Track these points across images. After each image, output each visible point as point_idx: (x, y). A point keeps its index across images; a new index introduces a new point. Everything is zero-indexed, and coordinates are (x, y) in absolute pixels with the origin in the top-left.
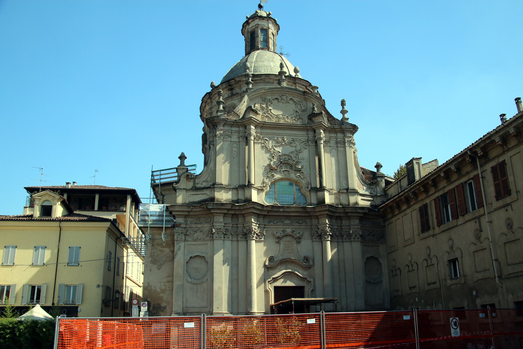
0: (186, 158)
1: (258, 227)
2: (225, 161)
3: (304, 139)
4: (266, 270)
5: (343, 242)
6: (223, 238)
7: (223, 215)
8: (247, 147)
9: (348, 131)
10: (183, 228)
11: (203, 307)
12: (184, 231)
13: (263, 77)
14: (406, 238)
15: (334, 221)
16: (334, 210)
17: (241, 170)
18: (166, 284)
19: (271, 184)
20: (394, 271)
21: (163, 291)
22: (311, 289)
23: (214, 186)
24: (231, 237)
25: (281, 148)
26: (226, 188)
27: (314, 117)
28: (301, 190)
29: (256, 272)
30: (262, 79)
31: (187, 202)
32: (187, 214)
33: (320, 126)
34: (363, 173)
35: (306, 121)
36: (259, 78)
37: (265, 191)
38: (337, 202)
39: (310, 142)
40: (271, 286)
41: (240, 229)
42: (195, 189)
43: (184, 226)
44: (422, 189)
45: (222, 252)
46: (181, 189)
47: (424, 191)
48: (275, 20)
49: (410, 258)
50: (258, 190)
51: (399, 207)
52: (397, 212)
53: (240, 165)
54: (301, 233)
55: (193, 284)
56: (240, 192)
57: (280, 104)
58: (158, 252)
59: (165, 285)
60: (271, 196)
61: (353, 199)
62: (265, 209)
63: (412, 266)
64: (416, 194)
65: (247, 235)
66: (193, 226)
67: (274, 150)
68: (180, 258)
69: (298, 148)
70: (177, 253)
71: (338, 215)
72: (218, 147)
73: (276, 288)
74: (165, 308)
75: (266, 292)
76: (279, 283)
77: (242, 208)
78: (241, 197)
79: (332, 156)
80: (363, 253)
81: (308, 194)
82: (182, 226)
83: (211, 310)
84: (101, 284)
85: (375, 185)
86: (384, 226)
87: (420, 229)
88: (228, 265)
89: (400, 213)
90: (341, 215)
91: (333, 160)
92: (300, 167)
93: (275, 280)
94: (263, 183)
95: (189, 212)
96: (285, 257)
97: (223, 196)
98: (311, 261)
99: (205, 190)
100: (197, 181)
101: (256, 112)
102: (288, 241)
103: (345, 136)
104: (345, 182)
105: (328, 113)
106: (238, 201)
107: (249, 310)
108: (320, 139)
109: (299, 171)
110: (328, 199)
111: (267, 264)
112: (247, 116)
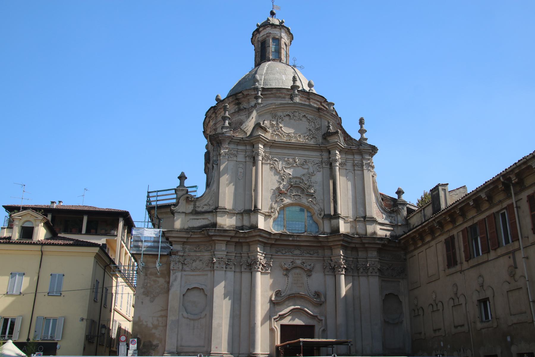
0: (186, 178)
1: (265, 257)
2: (230, 183)
3: (318, 160)
5: (359, 276)
6: (225, 269)
8: (254, 168)
9: (366, 153)
10: (180, 256)
11: (200, 346)
12: (182, 260)
13: (274, 91)
15: (349, 252)
16: (349, 240)
18: (160, 319)
19: (280, 209)
20: (416, 311)
21: (156, 327)
22: (322, 329)
23: (216, 210)
24: (233, 267)
25: (292, 170)
27: (329, 136)
28: (313, 217)
29: (261, 307)
30: (272, 94)
31: (186, 227)
32: (185, 240)
33: (336, 146)
34: (382, 199)
35: (320, 140)
36: (270, 93)
38: (353, 231)
39: (324, 164)
40: (277, 324)
41: (244, 259)
42: (195, 213)
43: (182, 254)
44: (448, 219)
45: (223, 284)
46: (179, 212)
47: (450, 221)
49: (434, 296)
50: (266, 215)
51: (422, 239)
52: (420, 244)
53: (247, 187)
54: (312, 265)
55: (190, 319)
56: (246, 217)
57: (292, 121)
58: (152, 283)
59: (158, 320)
61: (370, 229)
62: (272, 237)
63: (437, 305)
64: (441, 225)
65: (251, 266)
66: (192, 254)
67: (284, 171)
68: (176, 290)
69: (311, 170)
71: (353, 245)
72: (222, 167)
73: (282, 326)
74: (157, 346)
75: (272, 330)
76: (286, 321)
77: (246, 236)
78: (246, 223)
79: (348, 180)
81: (321, 221)
82: (180, 254)
83: (209, 351)
84: (85, 317)
85: (395, 214)
86: (405, 259)
87: (446, 264)
88: (229, 299)
89: (423, 245)
90: (357, 246)
91: (349, 184)
92: (312, 191)
93: (282, 317)
94: (271, 208)
95: (188, 238)
96: (293, 292)
97: (227, 222)
98: (323, 297)
99: (206, 214)
101: (265, 130)
102: (297, 274)
103: (363, 158)
104: (362, 209)
105: (344, 132)
106: (242, 228)
107: (251, 351)
108: (336, 161)
109: (311, 195)
110: (343, 228)
111: (273, 299)
112: (256, 134)
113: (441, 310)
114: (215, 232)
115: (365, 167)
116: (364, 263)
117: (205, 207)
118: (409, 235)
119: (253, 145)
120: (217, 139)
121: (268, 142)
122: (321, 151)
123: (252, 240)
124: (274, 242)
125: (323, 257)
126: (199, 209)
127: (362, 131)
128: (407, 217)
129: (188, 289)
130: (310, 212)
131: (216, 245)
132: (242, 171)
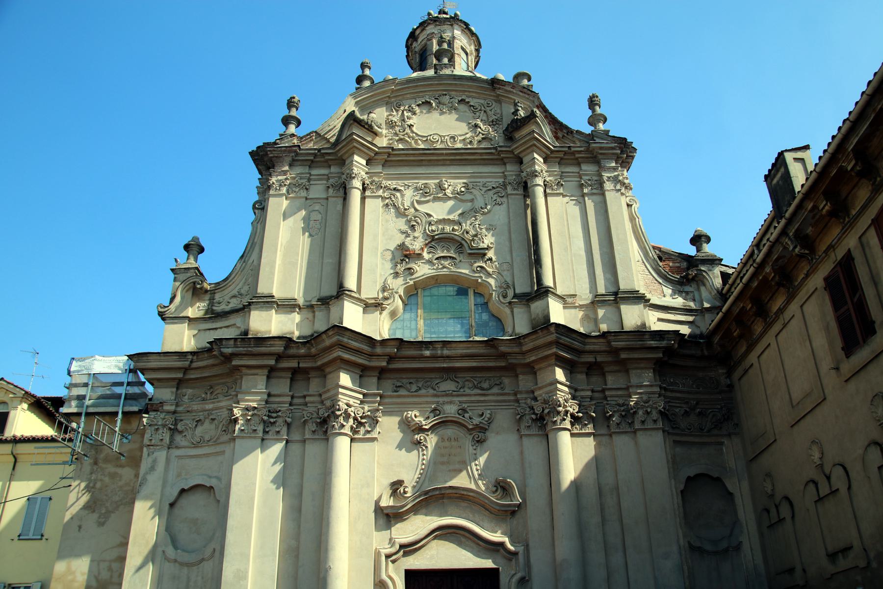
4: (382, 521)
6: (261, 434)
7: (266, 372)
9: (609, 157)
10: (168, 412)
12: (170, 419)
14: (797, 395)
15: (582, 377)
16: (576, 344)
19: (407, 290)
20: (773, 511)
22: (519, 575)
24: (285, 429)
26: (287, 306)
28: (490, 305)
33: (535, 145)
34: (660, 258)
37: (389, 309)
39: (509, 188)
40: (396, 570)
43: (173, 408)
44: (825, 207)
47: (832, 214)
48: (467, 25)
49: (816, 455)
51: (762, 311)
52: (758, 328)
54: (487, 414)
55: (183, 564)
56: (320, 314)
58: (107, 479)
59: (110, 569)
60: (407, 323)
61: (632, 316)
62: (379, 350)
63: (828, 478)
64: (807, 243)
65: (325, 425)
67: (416, 210)
70: (145, 479)
71: (590, 359)
73: (411, 576)
76: (420, 561)
77: (313, 350)
78: (321, 327)
80: (674, 464)
81: (507, 311)
82: (167, 408)
85: (694, 285)
86: (731, 387)
87: (839, 343)
89: (768, 326)
90: (599, 359)
94: (384, 289)
97: (269, 323)
100: (217, 297)
101: (369, 128)
102: (449, 439)
103: (601, 168)
105: (552, 120)
108: (534, 174)
113: (843, 490)
114: (236, 346)
115: (608, 186)
116: (621, 401)
118: (729, 310)
119: (343, 162)
120: (266, 159)
121: (376, 153)
122: (503, 162)
123: (325, 360)
124: (384, 364)
125: (515, 394)
126: (218, 308)
127: (594, 120)
128: (723, 289)
129: (183, 491)
130: (481, 295)
131: (244, 378)
132: (319, 217)
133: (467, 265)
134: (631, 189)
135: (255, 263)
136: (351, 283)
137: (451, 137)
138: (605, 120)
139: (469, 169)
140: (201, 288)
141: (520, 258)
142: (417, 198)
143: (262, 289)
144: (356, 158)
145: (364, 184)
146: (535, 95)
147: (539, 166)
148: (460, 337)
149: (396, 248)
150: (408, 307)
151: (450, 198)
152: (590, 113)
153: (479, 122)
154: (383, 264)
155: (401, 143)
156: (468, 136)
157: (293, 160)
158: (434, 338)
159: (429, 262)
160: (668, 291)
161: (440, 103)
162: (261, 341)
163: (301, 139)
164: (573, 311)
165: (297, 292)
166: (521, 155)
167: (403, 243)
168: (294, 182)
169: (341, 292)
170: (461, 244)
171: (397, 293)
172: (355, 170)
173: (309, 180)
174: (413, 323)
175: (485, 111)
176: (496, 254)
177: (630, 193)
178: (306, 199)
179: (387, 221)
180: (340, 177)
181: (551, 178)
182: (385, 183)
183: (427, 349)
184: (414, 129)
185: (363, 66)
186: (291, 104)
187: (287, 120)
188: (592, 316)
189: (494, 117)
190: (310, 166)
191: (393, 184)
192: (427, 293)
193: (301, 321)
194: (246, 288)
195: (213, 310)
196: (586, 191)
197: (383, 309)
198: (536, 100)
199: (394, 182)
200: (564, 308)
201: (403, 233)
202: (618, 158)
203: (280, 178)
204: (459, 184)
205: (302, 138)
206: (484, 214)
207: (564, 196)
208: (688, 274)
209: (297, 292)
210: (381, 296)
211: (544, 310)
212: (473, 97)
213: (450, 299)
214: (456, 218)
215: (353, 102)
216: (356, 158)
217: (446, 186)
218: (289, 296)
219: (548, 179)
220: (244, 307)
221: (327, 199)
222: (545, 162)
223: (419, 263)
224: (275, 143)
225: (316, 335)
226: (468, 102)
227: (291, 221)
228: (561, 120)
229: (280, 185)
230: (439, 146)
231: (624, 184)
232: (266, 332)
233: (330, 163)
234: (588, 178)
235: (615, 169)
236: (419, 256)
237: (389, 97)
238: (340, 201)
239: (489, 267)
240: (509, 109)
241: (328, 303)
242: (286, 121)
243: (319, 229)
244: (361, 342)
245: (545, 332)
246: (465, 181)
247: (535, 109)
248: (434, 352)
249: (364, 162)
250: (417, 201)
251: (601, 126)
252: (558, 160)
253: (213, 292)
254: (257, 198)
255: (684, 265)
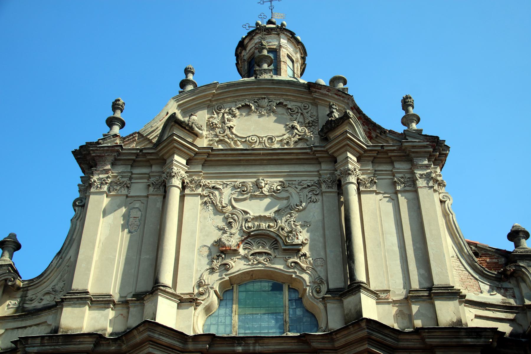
16: (389, 341)
17: (143, 257)
19: (222, 285)
26: (102, 302)
28: (304, 300)
37: (204, 304)
39: (324, 186)
48: (293, 34)
61: (447, 312)
67: (234, 208)
78: (133, 322)
81: (321, 306)
94: (200, 284)
97: (80, 320)
101: (189, 129)
103: (414, 166)
115: (421, 183)
117: (48, 297)
120: (88, 158)
121: (196, 153)
122: (317, 161)
127: (406, 120)
132: (139, 214)
133: (282, 261)
134: (444, 186)
135: (72, 259)
136: (166, 278)
137: (269, 139)
138: (418, 120)
139: (286, 169)
140: (13, 286)
141: (334, 254)
142: (235, 196)
143: (76, 285)
144: (176, 157)
145: (183, 183)
146: (350, 98)
147: (352, 164)
148: (274, 332)
149: (213, 245)
150: (223, 303)
151: (266, 196)
152: (403, 113)
153: (295, 124)
154: (200, 260)
155: (221, 144)
156: (285, 137)
157: (116, 159)
158: (248, 333)
159: (245, 258)
160: (485, 287)
161: (259, 106)
162: (71, 338)
163: (123, 139)
164: (386, 306)
165: (113, 288)
166: (335, 155)
167: (220, 239)
168: (115, 180)
169: (156, 288)
170: (276, 240)
171: (212, 288)
172: (175, 169)
173: (131, 178)
174: (228, 318)
175: (302, 114)
176: (311, 249)
177: (444, 190)
178: (127, 196)
179: (205, 218)
180: (160, 176)
181: (364, 176)
182: (204, 182)
183: (239, 345)
184: (234, 131)
185: (187, 71)
186: (116, 106)
187: (111, 121)
188: (406, 312)
189: (310, 119)
190: (134, 165)
191: (211, 182)
192: (242, 288)
193: (115, 317)
194: (61, 284)
195: (24, 307)
196: (398, 188)
197: (197, 305)
198: (350, 102)
199: (213, 181)
200: (377, 303)
201: (220, 229)
202: (430, 155)
203: (101, 176)
204: (275, 183)
205: (124, 138)
206: (299, 211)
207: (377, 193)
208: (505, 270)
209: (113, 288)
210: (196, 291)
211: (356, 305)
212: (290, 101)
213: (264, 294)
214: (272, 215)
215: (176, 105)
216: (176, 157)
217: (263, 185)
218: (104, 292)
219: (361, 177)
220: (57, 303)
221: (147, 197)
222: (358, 161)
223: (235, 259)
224: (98, 143)
225: (128, 330)
226: (286, 105)
227: (110, 217)
228: (375, 121)
229: (102, 184)
230: (257, 146)
231: (437, 181)
232: (77, 329)
233: (152, 162)
234: (400, 175)
235: (427, 167)
236: (235, 252)
237: (210, 100)
238: (160, 198)
239: (303, 263)
240: (324, 111)
241: (143, 299)
242: (111, 122)
243: (138, 226)
244: (173, 338)
245: (356, 327)
246: (281, 179)
247: (348, 111)
248: (246, 348)
249: (184, 162)
250: (235, 199)
251: (414, 126)
252: (372, 159)
253: (26, 289)
254: (78, 195)
255: (503, 260)
